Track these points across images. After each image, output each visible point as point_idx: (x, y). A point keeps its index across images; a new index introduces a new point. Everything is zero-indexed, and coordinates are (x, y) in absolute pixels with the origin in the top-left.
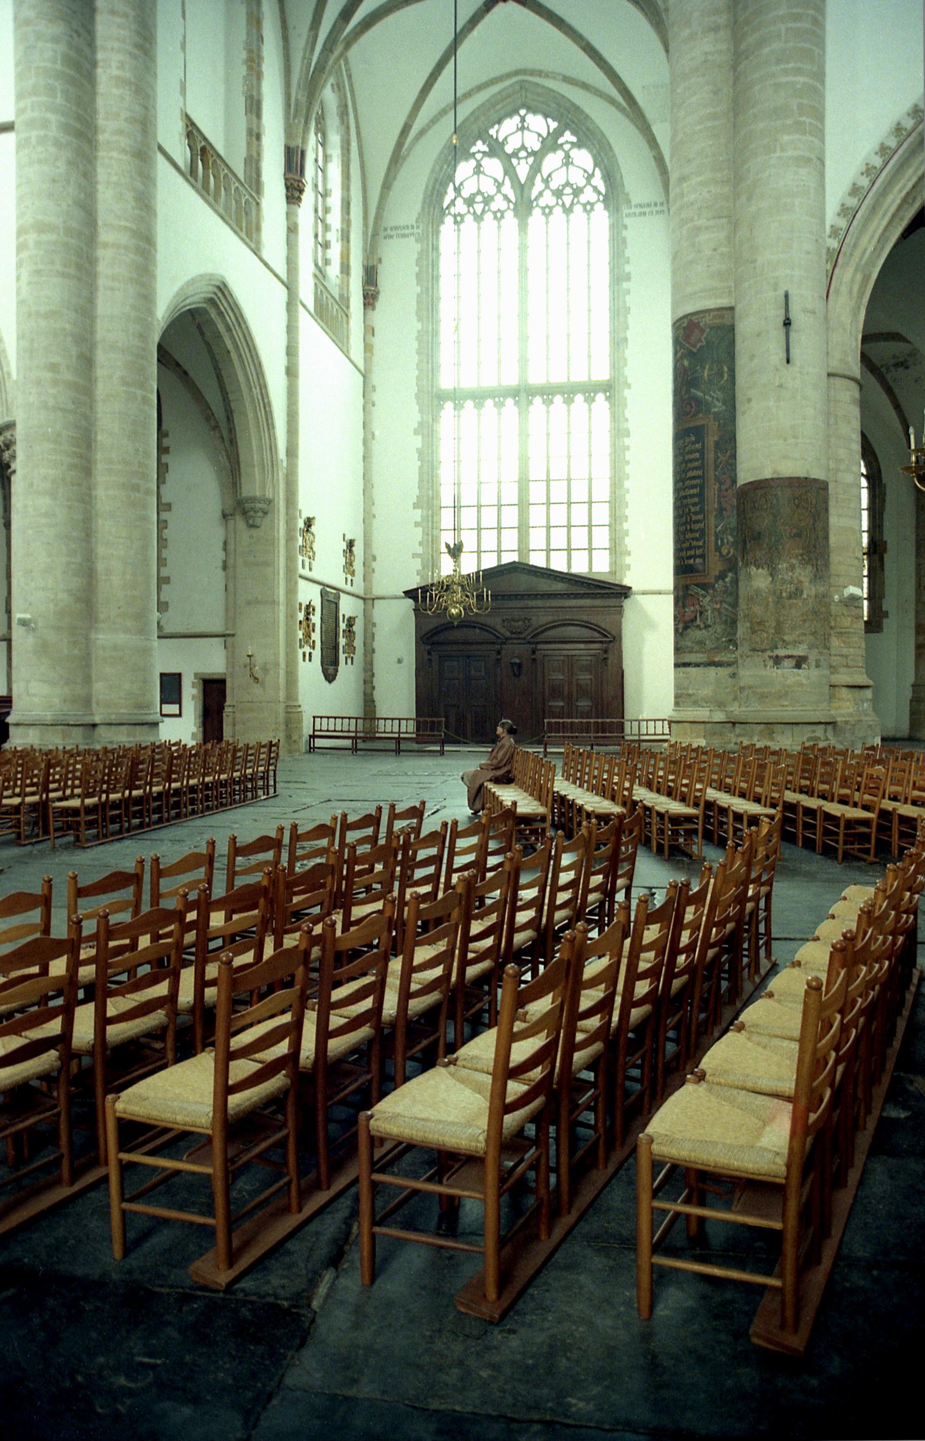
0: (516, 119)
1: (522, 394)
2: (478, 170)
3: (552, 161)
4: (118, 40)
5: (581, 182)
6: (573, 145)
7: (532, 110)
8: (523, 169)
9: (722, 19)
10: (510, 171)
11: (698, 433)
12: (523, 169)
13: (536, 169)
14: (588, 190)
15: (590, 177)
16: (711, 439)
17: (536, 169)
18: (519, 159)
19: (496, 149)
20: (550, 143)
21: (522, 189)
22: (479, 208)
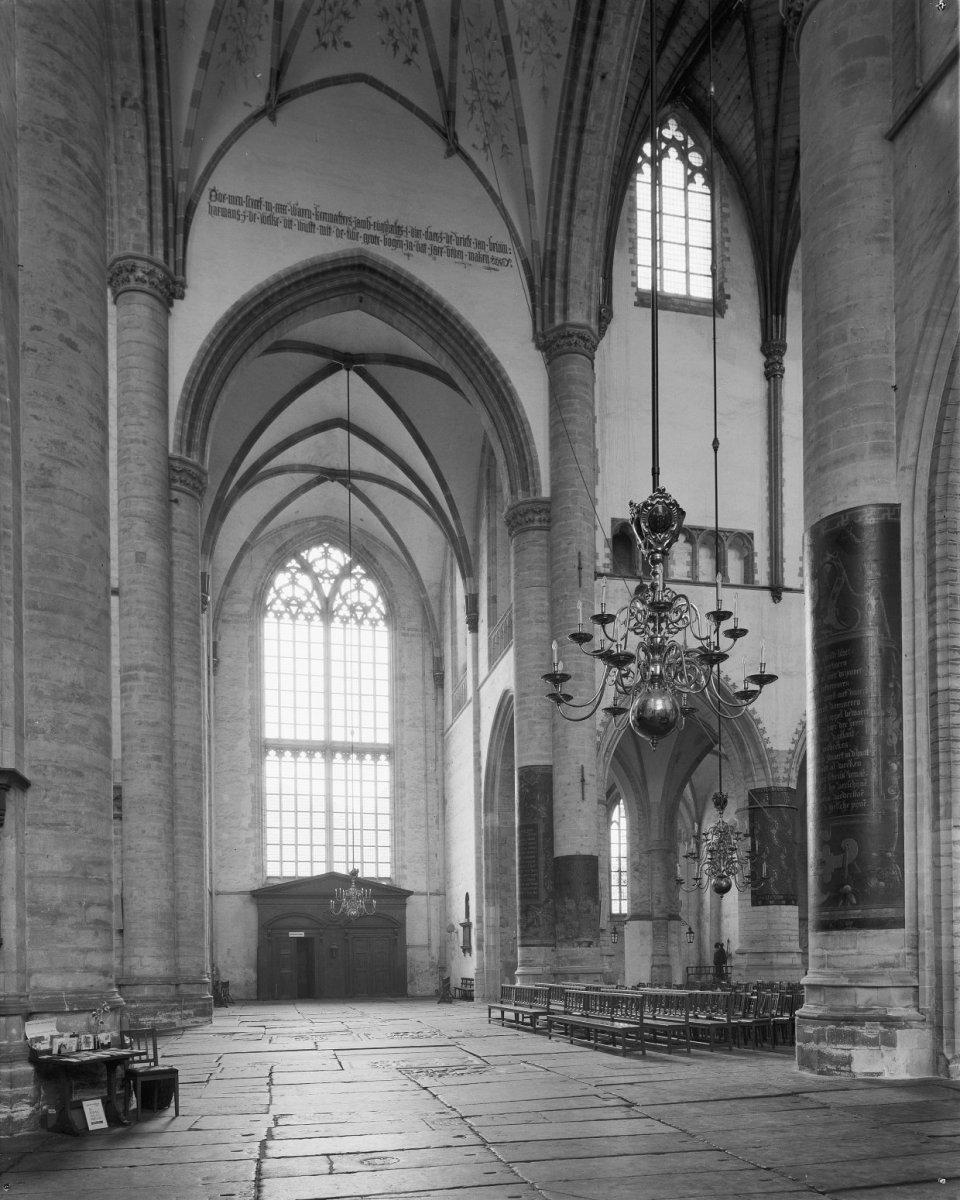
0: (321, 549)
1: (329, 749)
2: (293, 582)
3: (347, 585)
4: (186, 549)
5: (369, 604)
6: (364, 576)
7: (333, 544)
8: (327, 588)
9: (545, 618)
10: (317, 587)
11: (535, 828)
12: (327, 588)
13: (336, 589)
14: (373, 610)
15: (374, 601)
16: (541, 831)
17: (336, 589)
18: (324, 578)
19: (306, 568)
20: (346, 572)
21: (327, 602)
22: (294, 609)
